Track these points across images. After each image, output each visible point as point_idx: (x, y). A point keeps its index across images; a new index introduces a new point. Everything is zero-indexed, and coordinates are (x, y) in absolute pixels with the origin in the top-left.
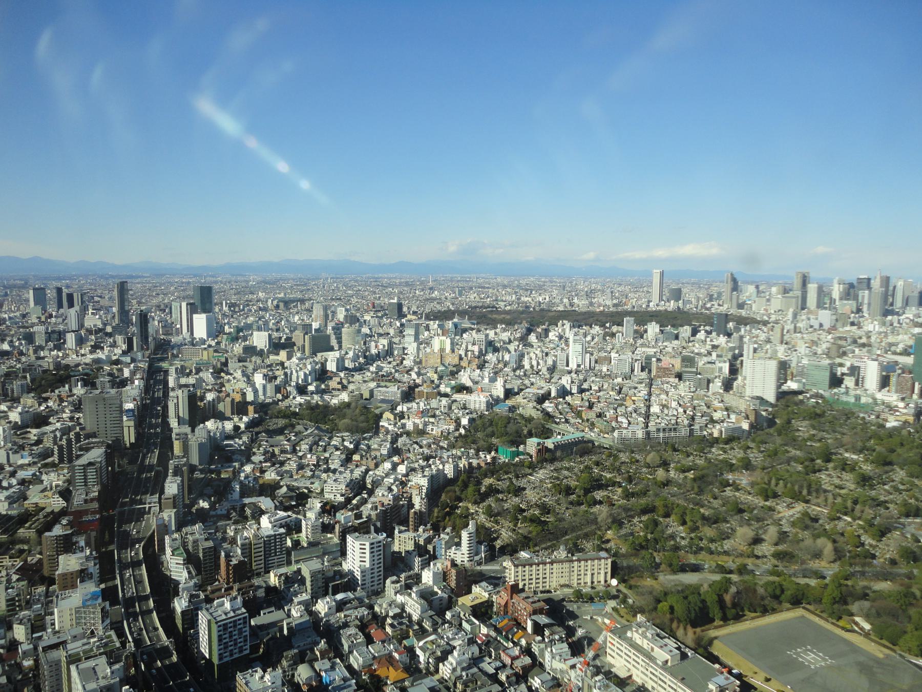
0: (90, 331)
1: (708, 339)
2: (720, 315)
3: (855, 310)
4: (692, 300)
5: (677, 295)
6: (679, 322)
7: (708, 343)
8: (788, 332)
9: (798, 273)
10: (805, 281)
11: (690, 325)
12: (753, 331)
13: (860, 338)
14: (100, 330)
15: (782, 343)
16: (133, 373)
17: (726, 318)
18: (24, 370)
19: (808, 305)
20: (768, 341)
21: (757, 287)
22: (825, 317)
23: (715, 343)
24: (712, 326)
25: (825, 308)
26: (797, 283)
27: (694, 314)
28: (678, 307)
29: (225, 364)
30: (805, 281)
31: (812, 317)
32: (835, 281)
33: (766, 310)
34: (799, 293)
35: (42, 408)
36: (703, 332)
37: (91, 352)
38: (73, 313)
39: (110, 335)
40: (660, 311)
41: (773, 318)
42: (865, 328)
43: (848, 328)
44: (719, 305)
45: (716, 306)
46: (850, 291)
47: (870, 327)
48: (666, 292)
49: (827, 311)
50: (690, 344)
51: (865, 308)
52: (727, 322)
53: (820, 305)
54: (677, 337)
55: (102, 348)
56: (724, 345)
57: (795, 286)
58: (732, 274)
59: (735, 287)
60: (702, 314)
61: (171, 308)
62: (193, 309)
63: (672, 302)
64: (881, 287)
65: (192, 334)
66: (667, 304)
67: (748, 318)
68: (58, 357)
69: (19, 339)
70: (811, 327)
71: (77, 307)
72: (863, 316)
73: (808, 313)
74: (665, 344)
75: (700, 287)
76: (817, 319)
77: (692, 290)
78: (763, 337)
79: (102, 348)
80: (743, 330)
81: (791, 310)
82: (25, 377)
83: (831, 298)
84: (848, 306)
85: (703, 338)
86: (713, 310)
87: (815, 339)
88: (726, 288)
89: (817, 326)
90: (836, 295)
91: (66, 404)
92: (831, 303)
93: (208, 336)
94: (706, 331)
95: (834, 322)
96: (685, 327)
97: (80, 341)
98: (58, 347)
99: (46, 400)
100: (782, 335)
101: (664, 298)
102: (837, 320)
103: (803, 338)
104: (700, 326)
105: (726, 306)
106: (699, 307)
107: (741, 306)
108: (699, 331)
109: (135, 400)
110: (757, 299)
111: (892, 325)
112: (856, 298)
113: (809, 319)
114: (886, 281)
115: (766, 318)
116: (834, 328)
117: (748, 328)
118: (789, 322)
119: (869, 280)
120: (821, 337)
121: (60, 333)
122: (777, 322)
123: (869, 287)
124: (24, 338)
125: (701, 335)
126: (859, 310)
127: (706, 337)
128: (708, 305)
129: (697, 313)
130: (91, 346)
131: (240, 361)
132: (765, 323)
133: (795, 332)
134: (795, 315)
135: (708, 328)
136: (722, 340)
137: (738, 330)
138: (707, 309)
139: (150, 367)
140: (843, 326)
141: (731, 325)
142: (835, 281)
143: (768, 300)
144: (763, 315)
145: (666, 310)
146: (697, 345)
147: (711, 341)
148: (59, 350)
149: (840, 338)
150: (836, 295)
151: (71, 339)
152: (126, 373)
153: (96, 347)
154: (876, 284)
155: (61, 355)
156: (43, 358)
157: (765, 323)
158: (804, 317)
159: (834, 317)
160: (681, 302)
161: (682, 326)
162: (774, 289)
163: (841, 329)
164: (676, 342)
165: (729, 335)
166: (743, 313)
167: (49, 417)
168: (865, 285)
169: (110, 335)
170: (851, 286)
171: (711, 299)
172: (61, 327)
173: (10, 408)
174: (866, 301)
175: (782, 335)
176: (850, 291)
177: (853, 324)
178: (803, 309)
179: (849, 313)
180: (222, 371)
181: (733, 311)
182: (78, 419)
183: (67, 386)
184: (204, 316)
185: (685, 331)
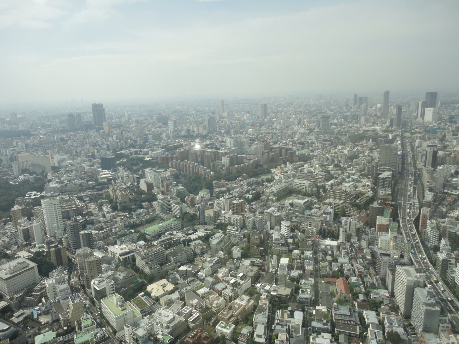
0: (370, 115)
14: (375, 115)
16: (395, 138)
18: (345, 132)
29: (445, 136)
35: (355, 150)
37: (372, 126)
38: (363, 106)
39: (379, 118)
55: (377, 124)
61: (409, 105)
62: (426, 105)
65: (423, 119)
68: (357, 127)
69: (340, 118)
71: (365, 104)
79: (377, 124)
82: (346, 135)
91: (365, 149)
93: (433, 120)
97: (367, 121)
98: (357, 123)
99: (357, 146)
109: (400, 150)
121: (357, 115)
124: (343, 118)
130: (372, 123)
131: (454, 135)
139: (402, 135)
148: (357, 124)
151: (363, 119)
152: (391, 137)
153: (374, 123)
155: (358, 126)
156: (351, 127)
167: (359, 154)
169: (379, 118)
172: (357, 113)
173: (343, 148)
180: (444, 140)
182: (372, 156)
183: (365, 141)
184: (431, 109)
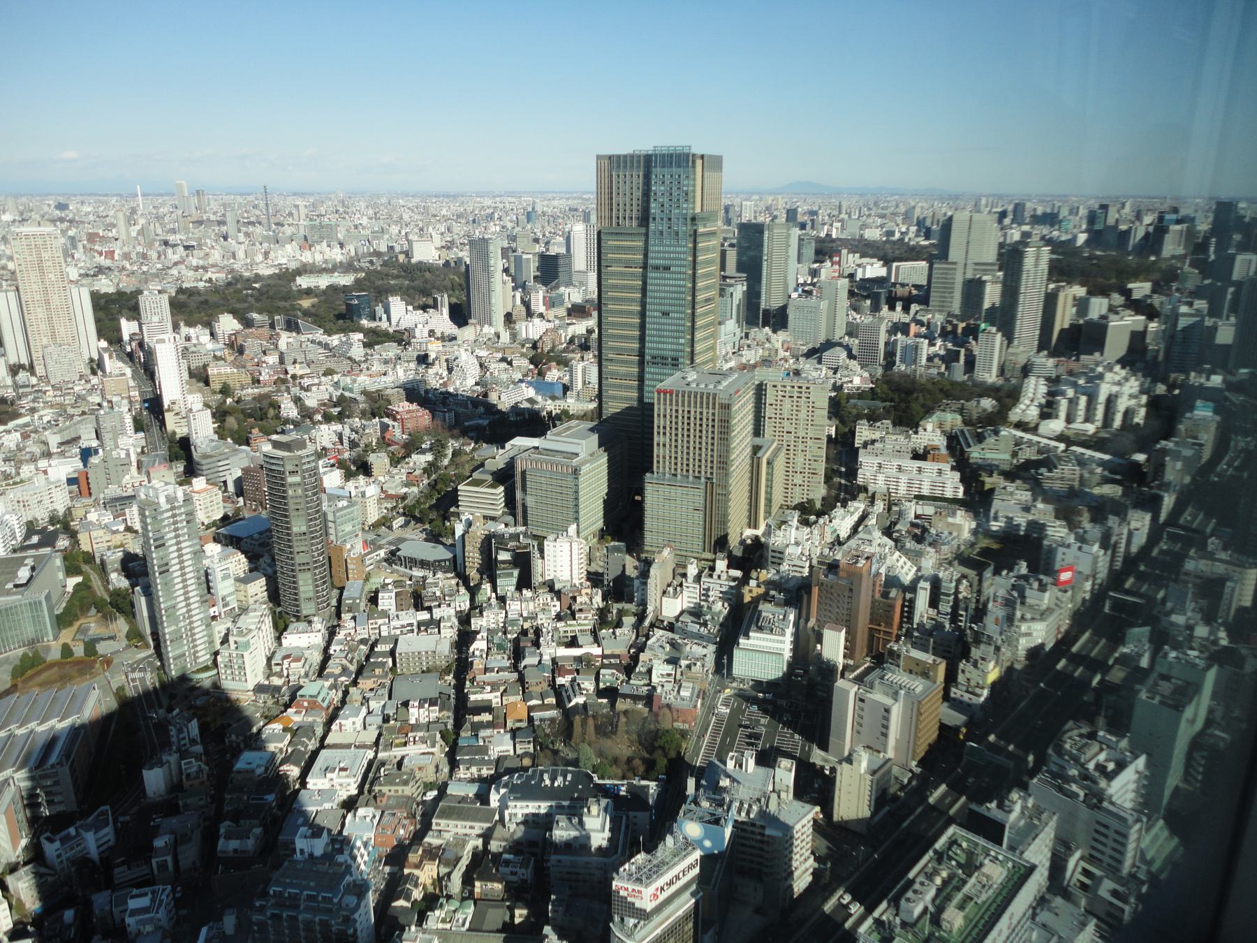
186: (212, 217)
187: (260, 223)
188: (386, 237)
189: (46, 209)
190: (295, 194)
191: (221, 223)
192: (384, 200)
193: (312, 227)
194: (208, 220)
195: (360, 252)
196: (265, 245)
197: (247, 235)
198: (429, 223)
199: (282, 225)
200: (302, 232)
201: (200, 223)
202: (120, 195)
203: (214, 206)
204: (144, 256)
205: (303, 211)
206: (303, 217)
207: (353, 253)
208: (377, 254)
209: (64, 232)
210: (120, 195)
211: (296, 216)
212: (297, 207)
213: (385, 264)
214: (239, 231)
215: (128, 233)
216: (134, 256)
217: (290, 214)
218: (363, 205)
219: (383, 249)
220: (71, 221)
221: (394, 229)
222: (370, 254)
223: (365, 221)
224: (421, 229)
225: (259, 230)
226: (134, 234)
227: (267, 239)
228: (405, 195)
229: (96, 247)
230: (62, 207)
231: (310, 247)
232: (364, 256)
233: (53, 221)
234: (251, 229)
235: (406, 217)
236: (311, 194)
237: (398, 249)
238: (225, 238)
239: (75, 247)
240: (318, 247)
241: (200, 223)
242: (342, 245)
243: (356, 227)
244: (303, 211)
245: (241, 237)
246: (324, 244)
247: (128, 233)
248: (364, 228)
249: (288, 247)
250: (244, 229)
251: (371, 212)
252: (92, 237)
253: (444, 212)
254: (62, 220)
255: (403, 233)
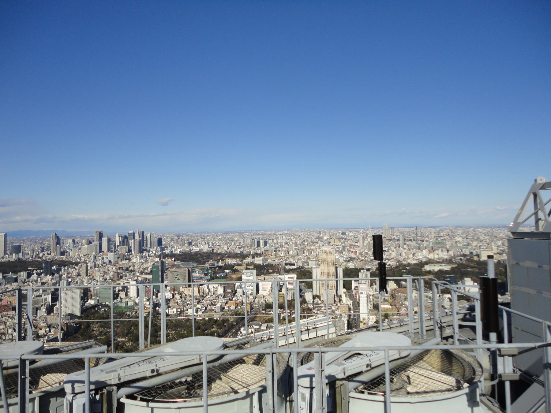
1: (39, 279)
2: (46, 262)
3: (127, 251)
4: (28, 253)
5: (17, 249)
6: (18, 269)
7: (39, 281)
8: (91, 268)
9: (96, 232)
10: (101, 236)
11: (25, 271)
12: (70, 270)
13: (130, 267)
15: (87, 275)
17: (50, 263)
19: (103, 250)
20: (79, 275)
21: (74, 241)
22: (111, 256)
23: (44, 281)
24: (42, 269)
25: (112, 252)
26: (96, 238)
27: (30, 262)
28: (19, 259)
30: (101, 236)
31: (104, 257)
32: (117, 235)
33: (79, 255)
34: (98, 243)
36: (35, 274)
40: (4, 262)
41: (83, 259)
42: (133, 261)
43: (124, 262)
44: (48, 254)
45: (46, 255)
46: (125, 239)
47: (135, 260)
48: (9, 247)
49: (113, 254)
50: (26, 284)
51: (133, 249)
52: (53, 266)
53: (109, 250)
54: (16, 280)
56: (50, 282)
57: (95, 239)
58: (56, 234)
59: (58, 242)
60: (36, 261)
63: (14, 255)
64: (139, 237)
66: (10, 256)
67: (66, 262)
70: (104, 263)
72: (132, 254)
73: (103, 255)
74: (6, 286)
75: (36, 242)
76: (107, 258)
77: (30, 245)
78: (75, 273)
80: (63, 270)
81: (93, 254)
83: (115, 245)
84: (123, 250)
85: (35, 278)
86: (44, 258)
87: (106, 270)
88: (53, 242)
89: (108, 263)
90: (118, 243)
92: (115, 248)
94: (37, 274)
95: (117, 259)
96: (22, 273)
100: (87, 270)
101: (8, 252)
102: (118, 258)
103: (99, 270)
104: (33, 270)
105: (53, 254)
106: (34, 257)
107: (62, 254)
108: (33, 274)
110: (72, 249)
111: (146, 257)
112: (128, 244)
113: (103, 259)
114: (142, 234)
115: (78, 260)
116: (116, 262)
117: (66, 268)
118: (92, 261)
119: (134, 233)
120: (110, 268)
122: (85, 262)
123: (134, 238)
125: (34, 277)
126: (130, 251)
127: (38, 278)
128: (41, 255)
129: (32, 261)
132: (77, 264)
133: (95, 267)
134: (95, 257)
135: (39, 271)
136: (49, 277)
137: (59, 270)
138: (40, 258)
140: (122, 260)
141: (54, 267)
142: (117, 235)
143: (80, 249)
144: (76, 258)
145: (9, 261)
146: (31, 284)
147: (41, 279)
149: (119, 268)
150: (118, 243)
154: (137, 235)
157: (77, 264)
158: (100, 258)
159: (117, 256)
160: (20, 254)
161: (21, 272)
162: (84, 241)
163: (120, 263)
164: (15, 284)
165: (53, 275)
166: (64, 258)
168: (132, 236)
170: (125, 237)
171: (43, 251)
174: (133, 246)
175: (87, 270)
176: (125, 239)
177: (126, 259)
178: (100, 252)
179: (125, 253)
181: (58, 257)
185: (23, 275)
186: (396, 238)
187: (414, 240)
188: (470, 247)
189: (338, 234)
190: (431, 227)
191: (398, 240)
192: (471, 229)
193: (435, 243)
194: (394, 239)
195: (456, 255)
196: (414, 250)
197: (408, 245)
198: (492, 241)
199: (423, 241)
200: (431, 245)
201: (390, 240)
202: (364, 229)
203: (397, 233)
204: (367, 254)
205: (433, 234)
206: (433, 237)
207: (452, 255)
208: (464, 256)
209: (342, 243)
210: (364, 229)
211: (430, 237)
212: (431, 233)
213: (468, 260)
214: (405, 244)
215: (363, 244)
216: (364, 253)
217: (428, 236)
218: (461, 232)
219: (467, 253)
220: (345, 239)
221: (475, 243)
222: (461, 256)
223: (460, 239)
224: (488, 244)
225: (413, 243)
226: (365, 245)
227: (415, 248)
228: (483, 227)
229: (352, 250)
230: (343, 234)
231: (434, 251)
232: (458, 256)
233: (339, 239)
234: (410, 242)
235: (481, 238)
236: (438, 227)
237: (475, 253)
238: (399, 247)
239: (344, 250)
240: (437, 252)
241: (390, 240)
242: (448, 251)
243: (456, 242)
244: (433, 235)
245: (405, 246)
246: (440, 250)
247: (363, 244)
248: (460, 243)
249: (424, 251)
250: (407, 243)
251: (464, 235)
252: (351, 246)
253: (501, 235)
254: (342, 238)
255: (479, 245)
